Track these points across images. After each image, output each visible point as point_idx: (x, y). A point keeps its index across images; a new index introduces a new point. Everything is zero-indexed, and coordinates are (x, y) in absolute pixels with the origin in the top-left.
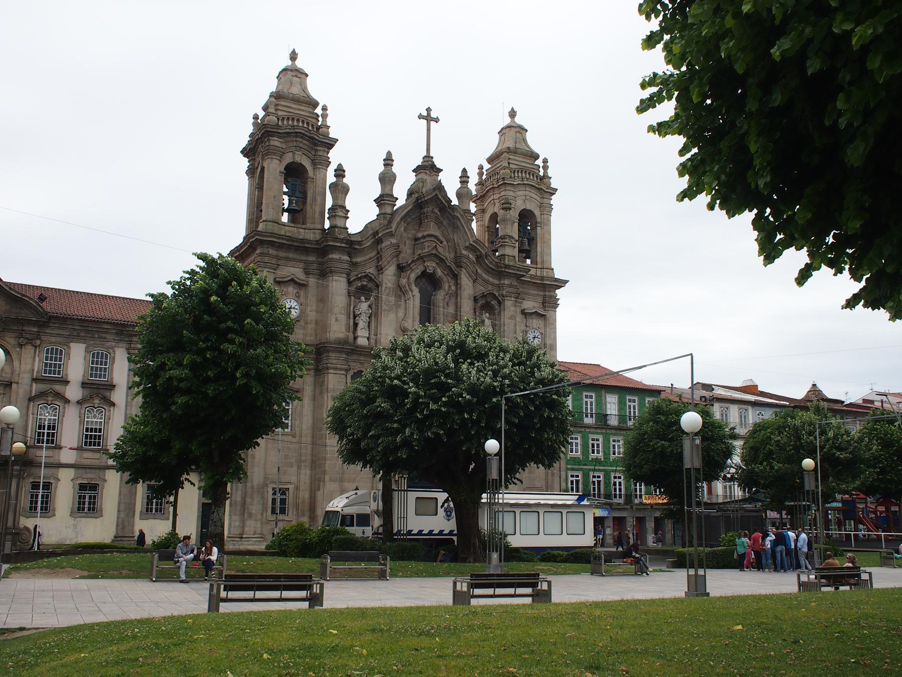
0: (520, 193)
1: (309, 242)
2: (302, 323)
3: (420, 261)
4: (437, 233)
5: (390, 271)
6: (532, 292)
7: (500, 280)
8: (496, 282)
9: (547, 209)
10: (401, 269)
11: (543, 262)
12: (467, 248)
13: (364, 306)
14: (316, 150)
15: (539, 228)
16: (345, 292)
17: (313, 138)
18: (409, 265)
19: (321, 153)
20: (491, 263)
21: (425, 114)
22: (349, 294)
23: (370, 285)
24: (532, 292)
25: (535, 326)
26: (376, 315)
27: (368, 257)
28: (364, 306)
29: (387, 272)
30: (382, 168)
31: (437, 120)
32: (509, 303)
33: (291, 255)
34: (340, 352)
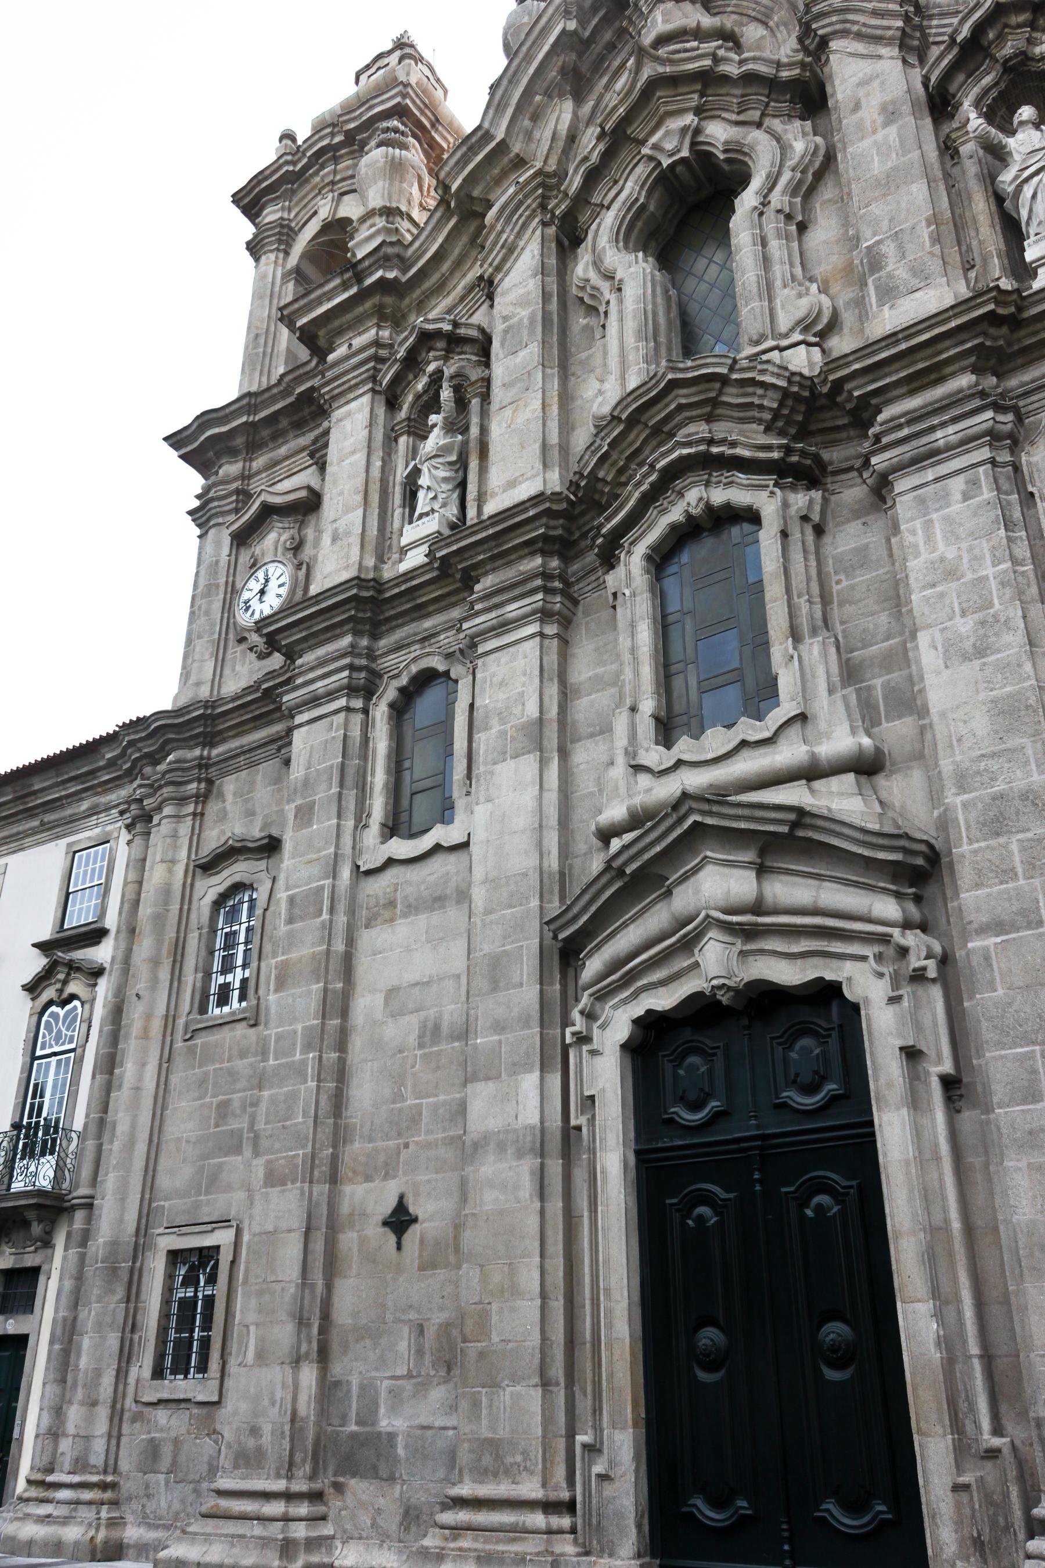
27: (459, 290)
28: (435, 439)
29: (507, 283)
33: (283, 451)
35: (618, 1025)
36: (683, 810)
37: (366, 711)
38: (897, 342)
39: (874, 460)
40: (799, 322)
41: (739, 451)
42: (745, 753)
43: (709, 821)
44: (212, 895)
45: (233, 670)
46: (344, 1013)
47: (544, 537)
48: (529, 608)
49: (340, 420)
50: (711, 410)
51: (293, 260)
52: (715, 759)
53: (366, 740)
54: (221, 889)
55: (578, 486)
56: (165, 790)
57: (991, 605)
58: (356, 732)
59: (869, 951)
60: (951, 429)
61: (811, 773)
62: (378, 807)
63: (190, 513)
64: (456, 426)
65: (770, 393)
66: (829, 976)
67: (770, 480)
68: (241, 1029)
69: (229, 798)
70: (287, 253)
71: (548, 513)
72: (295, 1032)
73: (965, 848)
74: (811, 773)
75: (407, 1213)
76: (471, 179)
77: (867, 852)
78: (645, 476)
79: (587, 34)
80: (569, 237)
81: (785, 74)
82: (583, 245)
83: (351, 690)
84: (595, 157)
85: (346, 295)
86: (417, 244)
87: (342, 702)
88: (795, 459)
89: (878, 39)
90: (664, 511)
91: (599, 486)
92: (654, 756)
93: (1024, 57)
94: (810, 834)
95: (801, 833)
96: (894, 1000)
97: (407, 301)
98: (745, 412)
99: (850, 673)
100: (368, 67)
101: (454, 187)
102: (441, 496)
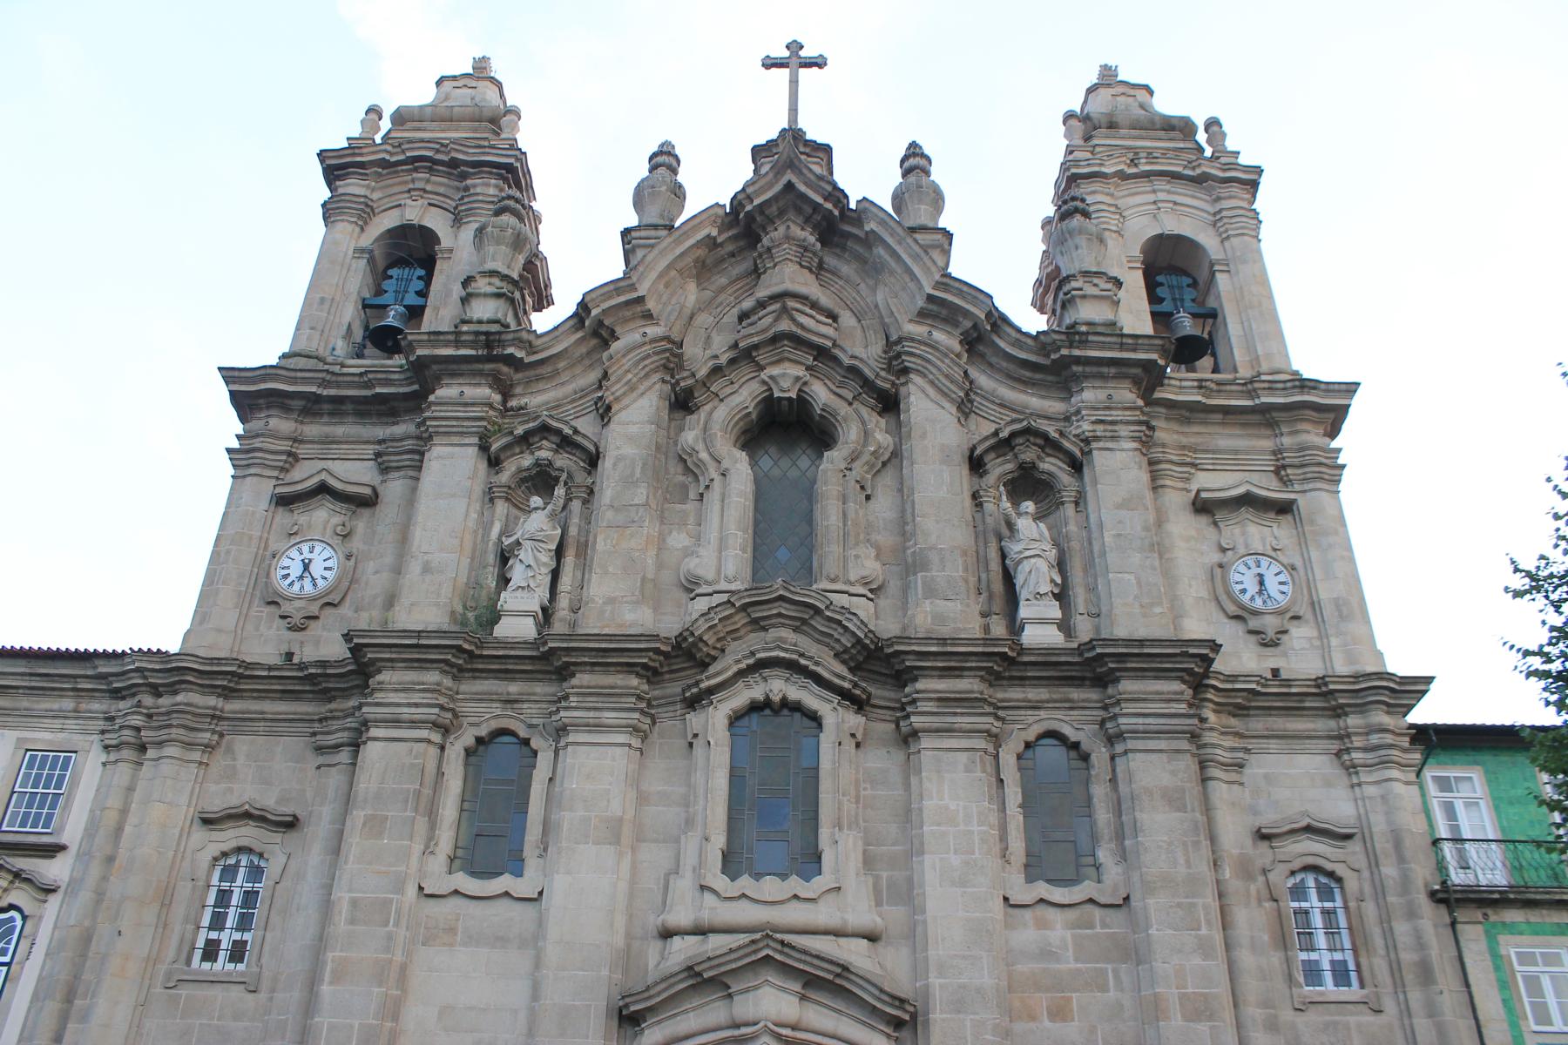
2: (346, 610)
3: (745, 371)
5: (639, 414)
6: (1223, 443)
7: (1067, 399)
8: (1055, 406)
10: (682, 403)
12: (923, 315)
14: (467, 189)
15: (1222, 280)
16: (479, 488)
17: (454, 163)
18: (704, 384)
19: (478, 190)
20: (1017, 344)
21: (786, 54)
22: (490, 496)
23: (563, 461)
24: (1223, 443)
26: (583, 550)
27: (569, 388)
28: (538, 522)
31: (818, 63)
33: (339, 430)
34: (423, 664)
36: (761, 945)
37: (442, 748)
38: (945, 645)
39: (913, 719)
41: (819, 670)
42: (795, 904)
43: (778, 957)
44: (214, 849)
45: (257, 629)
46: (395, 1018)
47: (644, 666)
50: (800, 626)
51: (367, 240)
52: (769, 901)
53: (440, 774)
54: (226, 847)
55: (685, 639)
56: (174, 730)
57: (973, 853)
58: (431, 767)
61: (838, 933)
62: (445, 840)
63: (229, 451)
65: (848, 635)
67: (836, 699)
68: (236, 992)
69: (241, 760)
70: (362, 229)
71: (657, 651)
72: (352, 1027)
74: (838, 933)
77: (879, 1005)
78: (745, 657)
79: (719, 240)
80: (682, 403)
82: (694, 417)
83: (436, 725)
84: (723, 360)
85: (473, 352)
87: (424, 733)
88: (857, 692)
90: (748, 686)
91: (701, 645)
92: (721, 882)
93: (1034, 466)
95: (838, 981)
98: (823, 639)
99: (868, 862)
100: (454, 78)
101: (594, 312)
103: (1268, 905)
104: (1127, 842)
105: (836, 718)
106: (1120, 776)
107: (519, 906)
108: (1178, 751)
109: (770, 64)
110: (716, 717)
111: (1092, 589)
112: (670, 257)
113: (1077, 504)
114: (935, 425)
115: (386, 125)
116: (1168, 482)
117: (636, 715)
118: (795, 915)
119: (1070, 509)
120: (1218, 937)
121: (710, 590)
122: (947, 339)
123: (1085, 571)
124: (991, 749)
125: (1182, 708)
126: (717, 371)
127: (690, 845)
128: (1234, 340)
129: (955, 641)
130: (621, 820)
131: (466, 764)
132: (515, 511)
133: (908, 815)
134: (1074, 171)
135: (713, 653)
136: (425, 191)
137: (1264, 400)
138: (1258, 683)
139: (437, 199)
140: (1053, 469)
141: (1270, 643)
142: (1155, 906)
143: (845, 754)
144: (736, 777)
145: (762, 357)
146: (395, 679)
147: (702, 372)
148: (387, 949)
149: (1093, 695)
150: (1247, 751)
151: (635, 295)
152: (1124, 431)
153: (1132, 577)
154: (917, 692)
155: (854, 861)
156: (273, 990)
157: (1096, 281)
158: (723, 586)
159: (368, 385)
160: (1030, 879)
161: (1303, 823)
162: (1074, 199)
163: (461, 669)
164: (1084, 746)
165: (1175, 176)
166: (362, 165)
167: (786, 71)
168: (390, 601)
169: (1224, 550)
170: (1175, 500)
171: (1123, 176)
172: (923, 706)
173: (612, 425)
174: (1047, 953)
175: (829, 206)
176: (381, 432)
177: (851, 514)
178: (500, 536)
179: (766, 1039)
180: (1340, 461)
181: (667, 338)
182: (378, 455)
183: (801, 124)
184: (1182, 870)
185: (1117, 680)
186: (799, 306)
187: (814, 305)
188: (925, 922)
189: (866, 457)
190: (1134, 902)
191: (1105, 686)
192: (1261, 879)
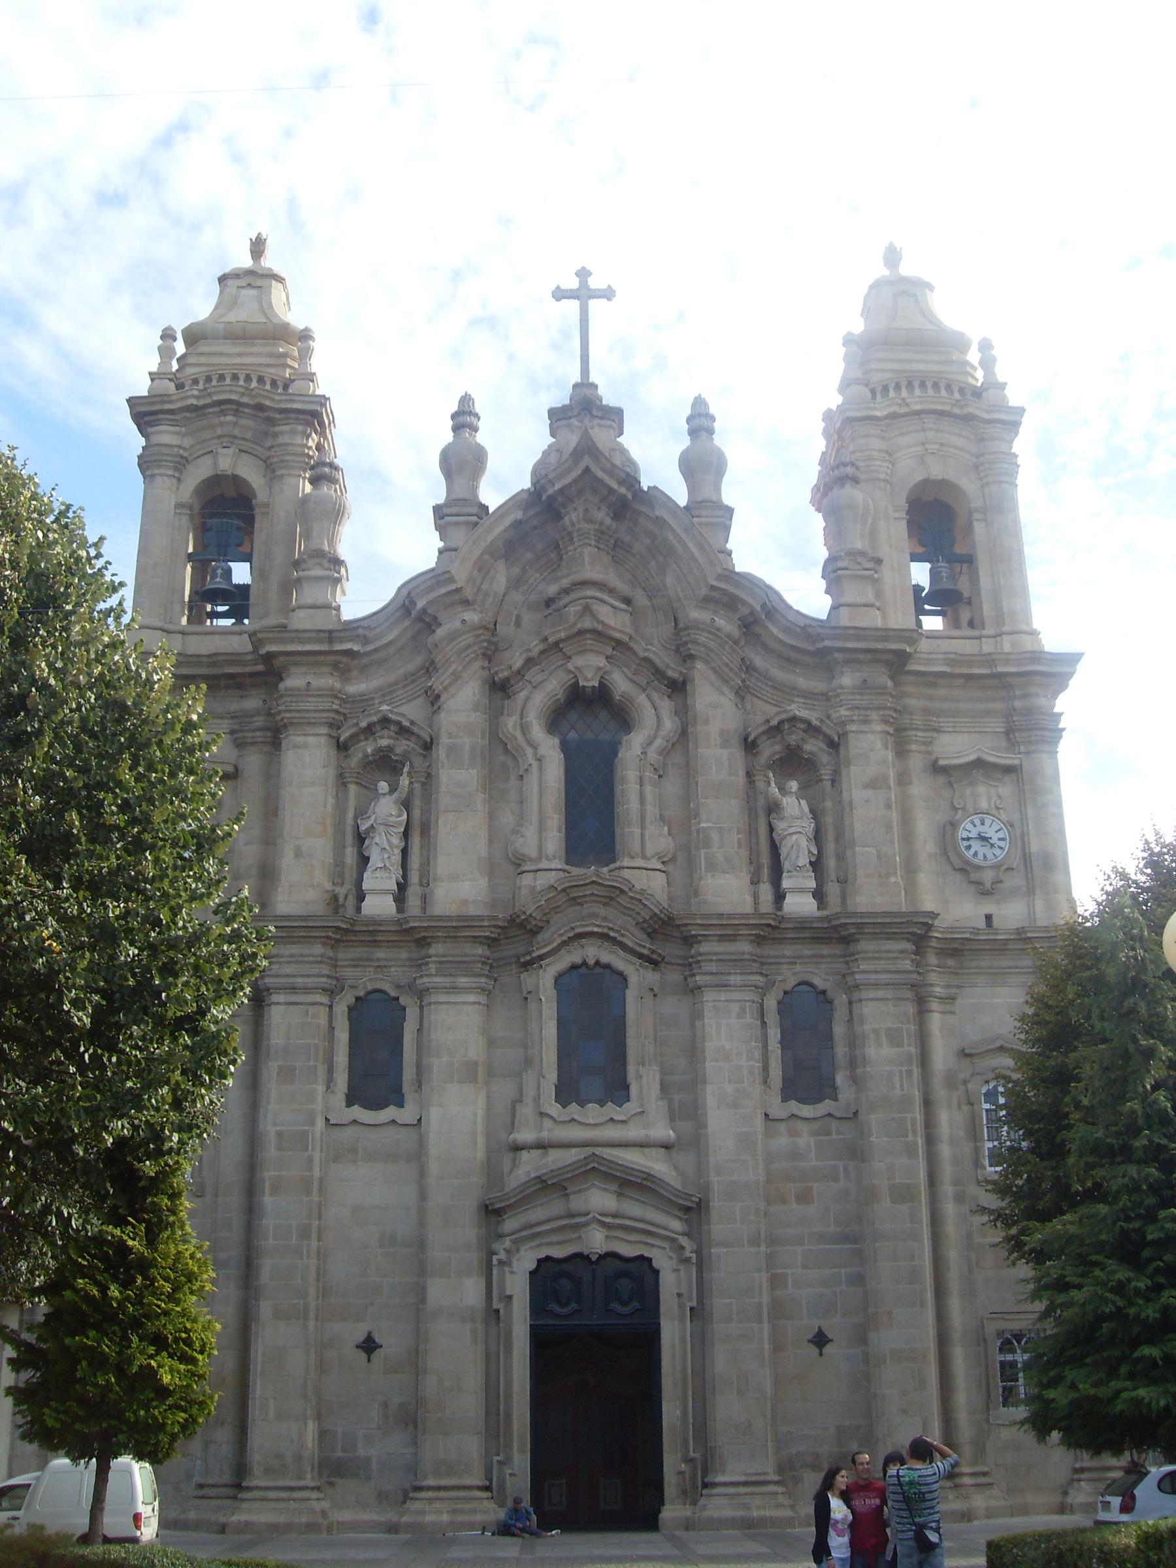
0: (908, 439)
1: (233, 658)
4: (612, 578)
9: (995, 469)
10: (500, 688)
11: (999, 620)
12: (706, 602)
13: (386, 808)
14: (275, 435)
15: (979, 529)
16: (332, 773)
17: (260, 407)
18: (520, 673)
22: (342, 781)
23: (403, 746)
25: (984, 805)
26: (426, 830)
27: (401, 672)
30: (448, 437)
31: (608, 294)
32: (869, 749)
35: (526, 1260)
37: (331, 1007)
39: (698, 978)
40: (657, 854)
41: (624, 940)
42: (610, 1125)
47: (487, 938)
48: (474, 985)
49: (296, 746)
50: (608, 901)
53: (332, 1028)
59: (666, 1245)
60: (739, 978)
64: (406, 804)
66: (646, 1255)
73: (716, 1204)
75: (374, 1341)
76: (430, 603)
81: (670, 673)
84: (535, 652)
86: (378, 630)
88: (654, 956)
89: (725, 681)
91: (531, 920)
92: (554, 1109)
93: (799, 747)
94: (649, 1184)
96: (676, 1271)
97: (356, 662)
99: (664, 1088)
102: (393, 858)
103: (965, 1108)
104: (859, 1071)
105: (638, 977)
106: (855, 1019)
107: (403, 1130)
108: (899, 999)
109: (560, 294)
110: (545, 979)
111: (841, 857)
112: (483, 545)
113: (833, 781)
114: (716, 708)
115: (180, 348)
116: (914, 747)
117: (483, 980)
118: (611, 1133)
119: (828, 785)
120: (920, 1141)
121: (533, 868)
122: (726, 624)
123: (837, 840)
124: (757, 999)
125: (907, 964)
126: (530, 662)
127: (530, 1080)
128: (984, 594)
129: (730, 916)
130: (476, 1064)
131: (350, 1019)
132: (365, 791)
133: (694, 1051)
134: (850, 414)
135: (540, 924)
136: (235, 437)
137: (1000, 669)
138: (971, 933)
139: (246, 445)
140: (814, 749)
141: (985, 892)
142: (875, 1120)
143: (643, 1010)
144: (562, 1023)
145: (568, 650)
146: (287, 952)
147: (518, 664)
148: (310, 1169)
149: (837, 950)
150: (959, 987)
151: (453, 587)
152: (874, 716)
153: (873, 850)
154: (701, 955)
155: (656, 1086)
156: (216, 1195)
157: (860, 560)
158: (544, 864)
159: (214, 665)
160: (785, 1099)
161: (998, 1044)
162: (845, 465)
163: (338, 941)
164: (829, 994)
165: (941, 413)
166: (171, 412)
167: (574, 305)
168: (267, 875)
169: (956, 809)
170: (916, 762)
171: (893, 416)
172: (707, 967)
173: (443, 715)
174: (795, 1155)
175: (623, 490)
176: (234, 706)
177: (649, 797)
178: (356, 817)
179: (594, 1225)
180: (1061, 726)
181: (486, 628)
182: (232, 732)
183: (594, 378)
184: (898, 1092)
185: (858, 940)
186: (598, 594)
187: (611, 591)
188: (706, 1135)
189: (658, 742)
190: (860, 1117)
191: (848, 943)
192: (962, 1088)
